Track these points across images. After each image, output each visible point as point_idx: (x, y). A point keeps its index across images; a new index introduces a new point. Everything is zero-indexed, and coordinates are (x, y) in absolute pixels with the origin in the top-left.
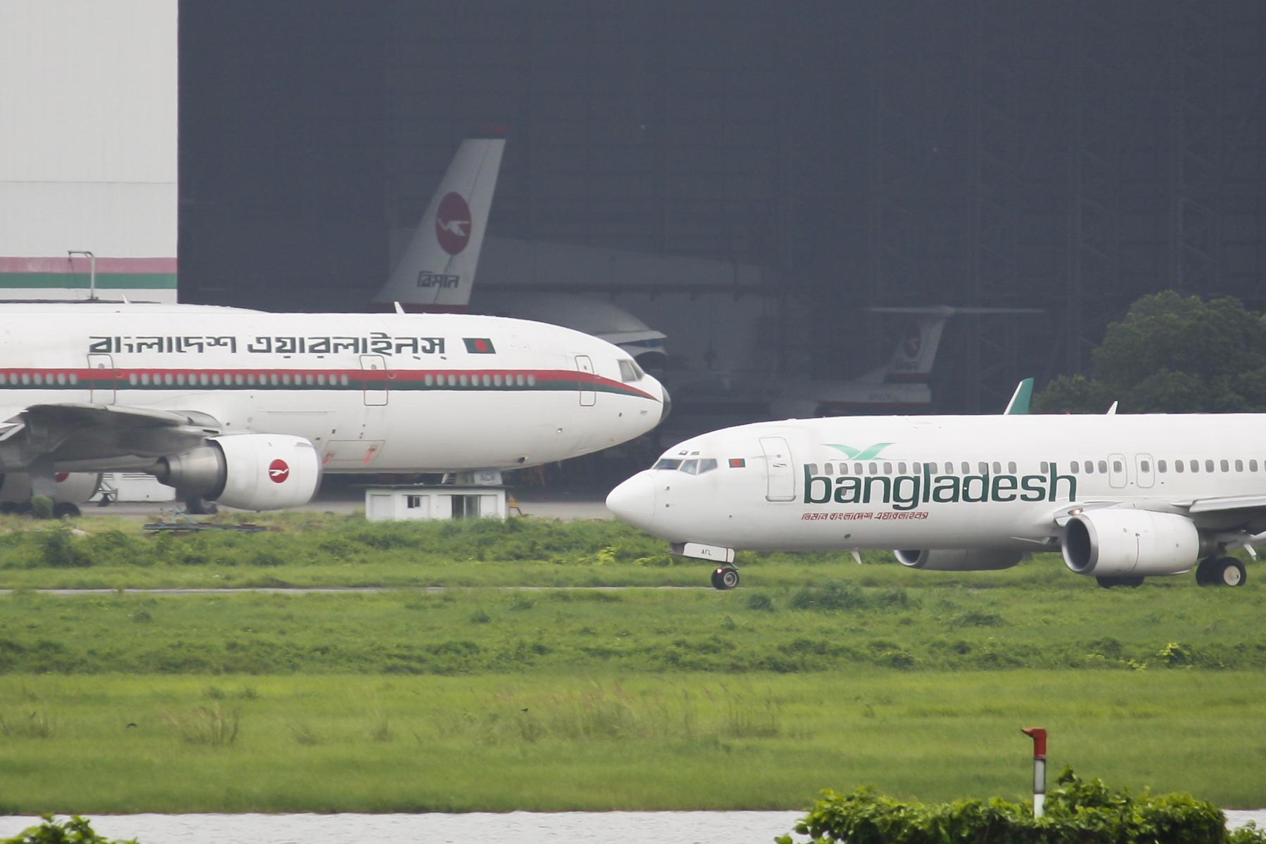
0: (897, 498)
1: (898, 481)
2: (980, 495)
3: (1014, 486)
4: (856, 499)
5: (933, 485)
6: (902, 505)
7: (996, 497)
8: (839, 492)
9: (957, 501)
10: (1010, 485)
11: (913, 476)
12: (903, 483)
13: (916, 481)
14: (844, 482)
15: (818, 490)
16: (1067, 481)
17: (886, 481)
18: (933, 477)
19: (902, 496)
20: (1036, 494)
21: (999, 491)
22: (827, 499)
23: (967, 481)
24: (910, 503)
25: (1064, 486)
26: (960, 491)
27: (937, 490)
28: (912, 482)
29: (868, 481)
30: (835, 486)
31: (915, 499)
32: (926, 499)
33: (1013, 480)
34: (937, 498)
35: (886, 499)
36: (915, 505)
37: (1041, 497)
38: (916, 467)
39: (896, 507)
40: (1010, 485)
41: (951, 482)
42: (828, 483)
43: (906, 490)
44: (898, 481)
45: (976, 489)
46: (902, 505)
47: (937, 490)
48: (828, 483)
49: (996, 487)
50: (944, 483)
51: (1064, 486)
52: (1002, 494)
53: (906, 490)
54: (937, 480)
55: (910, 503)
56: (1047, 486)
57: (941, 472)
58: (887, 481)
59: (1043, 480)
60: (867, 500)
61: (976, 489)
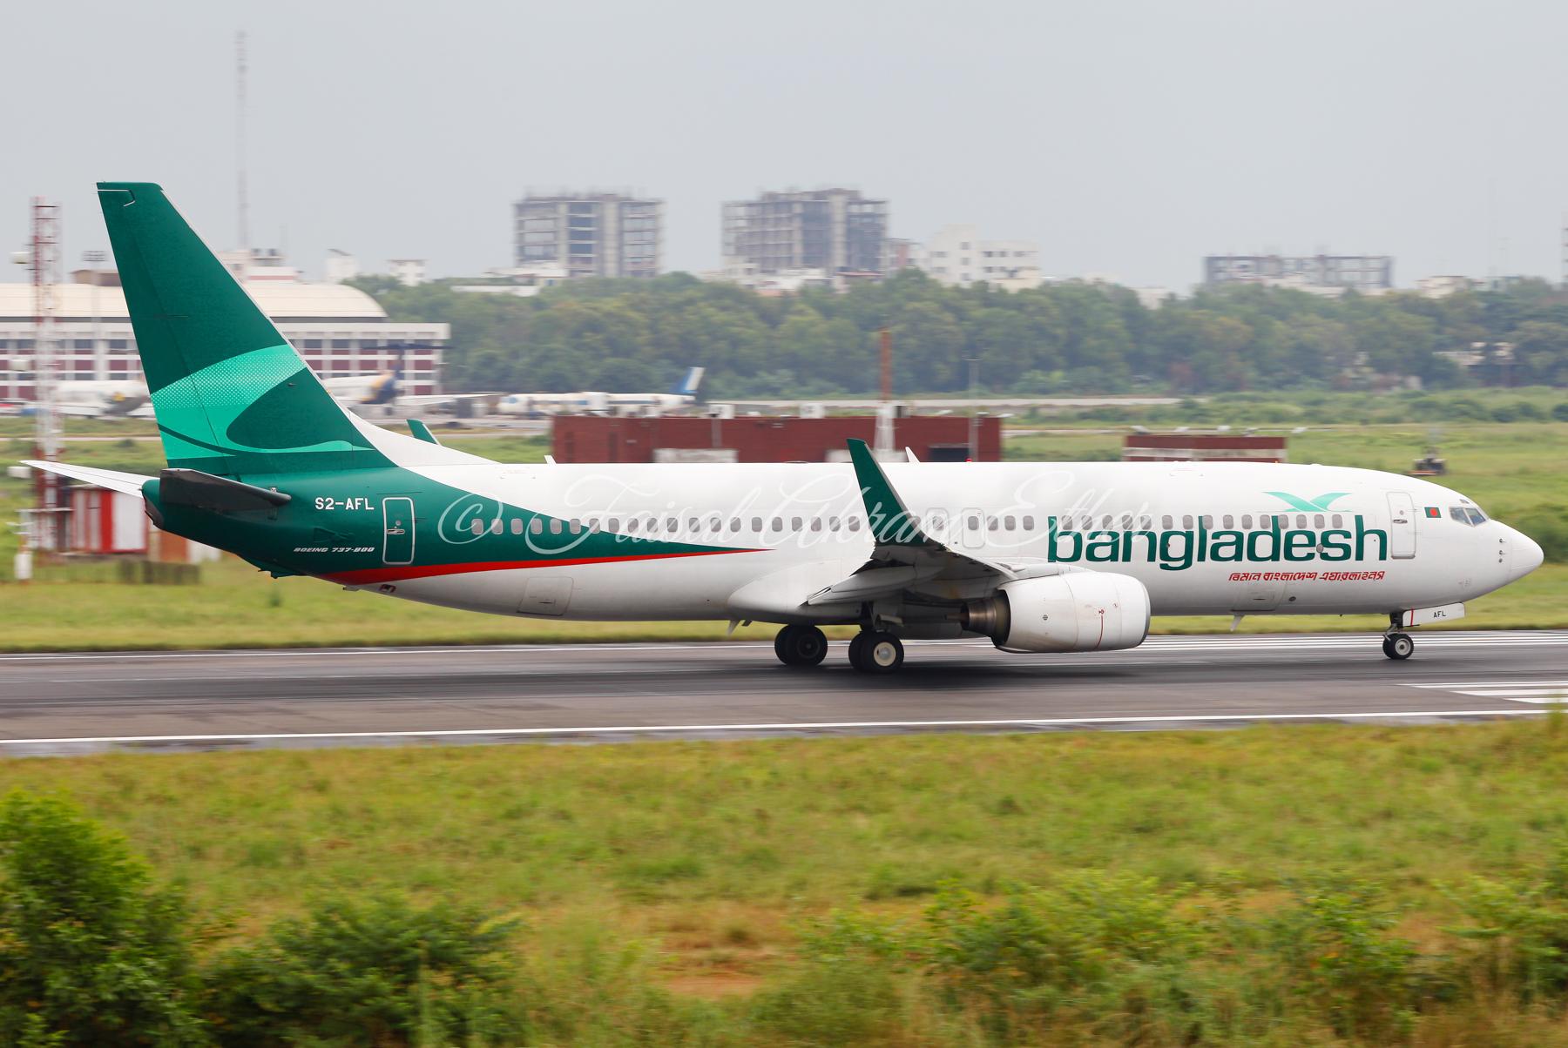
0: (1165, 556)
1: (1166, 537)
2: (1270, 554)
3: (1312, 543)
4: (1114, 557)
5: (1210, 542)
6: (1171, 564)
7: (1289, 556)
8: (1091, 548)
9: (1241, 560)
10: (1307, 543)
11: (1184, 531)
12: (1172, 540)
13: (1189, 537)
14: (1221, 537)
15: (1065, 546)
16: (1377, 537)
17: (1152, 537)
18: (1209, 534)
19: (1171, 554)
20: (1339, 552)
21: (1293, 549)
22: (1076, 557)
23: (1253, 537)
24: (1182, 563)
25: (1371, 543)
26: (1244, 547)
27: (1215, 548)
28: (1182, 539)
29: (1128, 536)
30: (1086, 542)
31: (1188, 559)
32: (1201, 558)
33: (1311, 536)
34: (1215, 556)
35: (1151, 558)
36: (1188, 564)
37: (1346, 556)
38: (1187, 521)
39: (1164, 567)
40: (1307, 543)
41: (1232, 538)
42: (1078, 539)
43: (1177, 547)
44: (1166, 537)
45: (1264, 546)
46: (1171, 564)
47: (1215, 548)
48: (1078, 539)
49: (1289, 545)
50: (1223, 539)
51: (1371, 543)
52: (1296, 552)
53: (1177, 547)
54: (1216, 536)
55: (1182, 563)
56: (1352, 542)
57: (1218, 526)
58: (1152, 537)
59: (1347, 535)
60: (1127, 558)
61: (1264, 546)
